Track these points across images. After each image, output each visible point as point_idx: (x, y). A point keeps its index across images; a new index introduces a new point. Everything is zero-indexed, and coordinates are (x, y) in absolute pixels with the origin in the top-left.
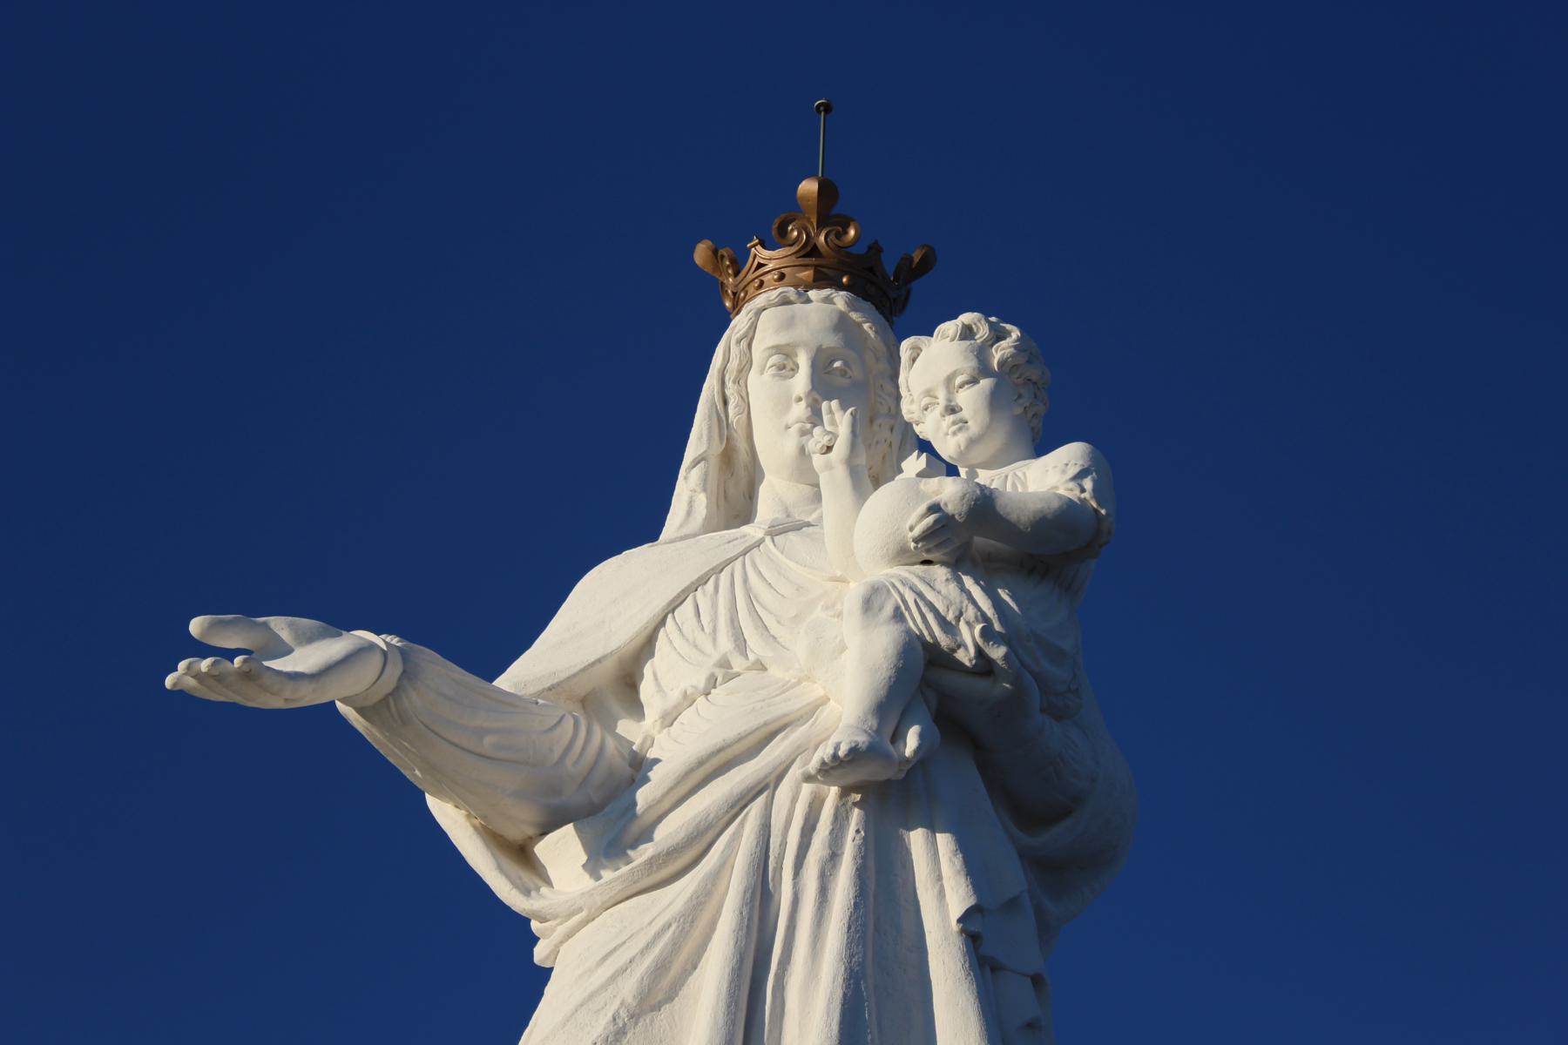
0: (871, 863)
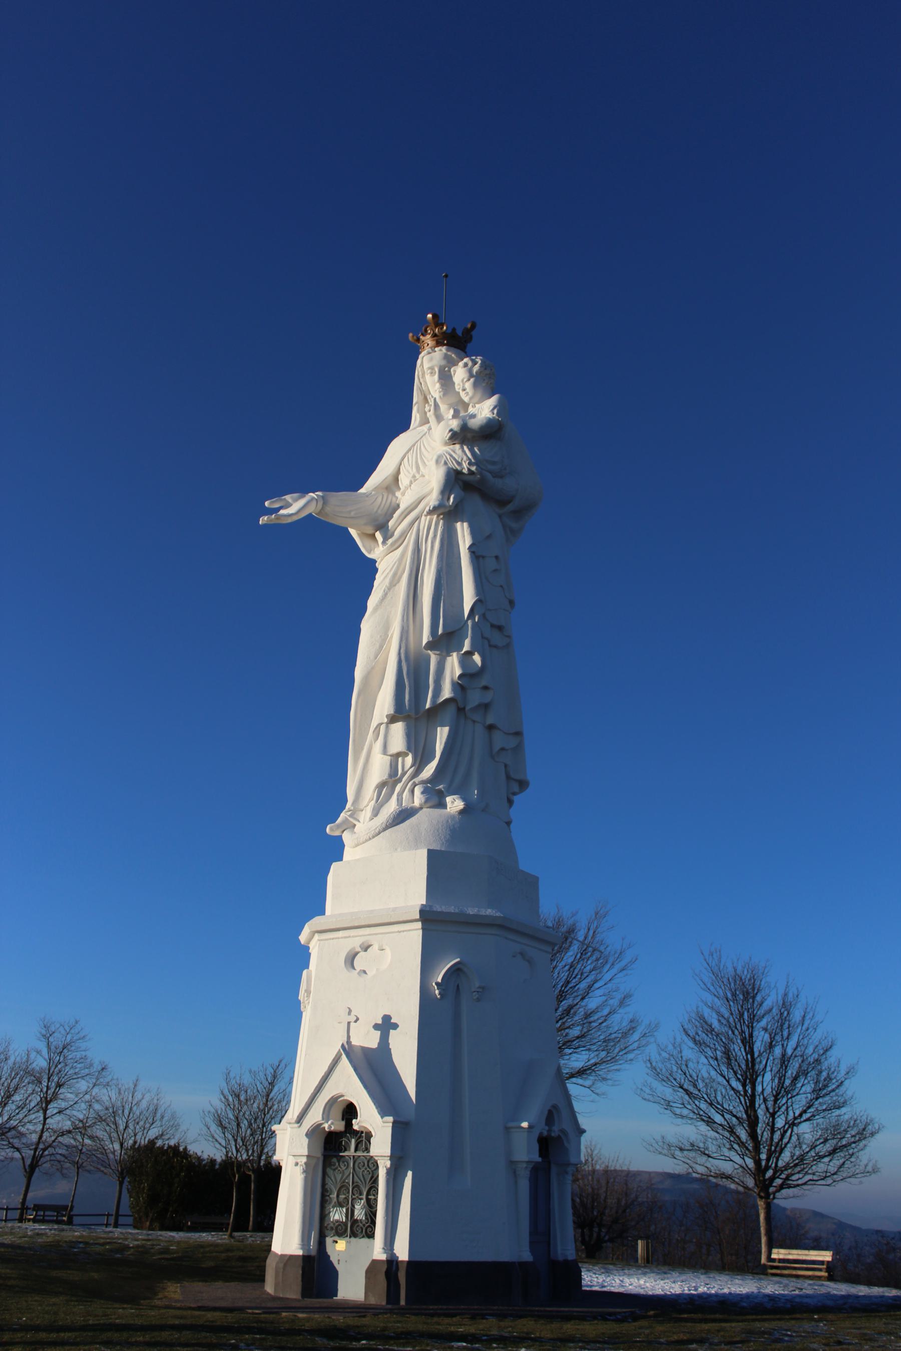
0: (446, 536)
